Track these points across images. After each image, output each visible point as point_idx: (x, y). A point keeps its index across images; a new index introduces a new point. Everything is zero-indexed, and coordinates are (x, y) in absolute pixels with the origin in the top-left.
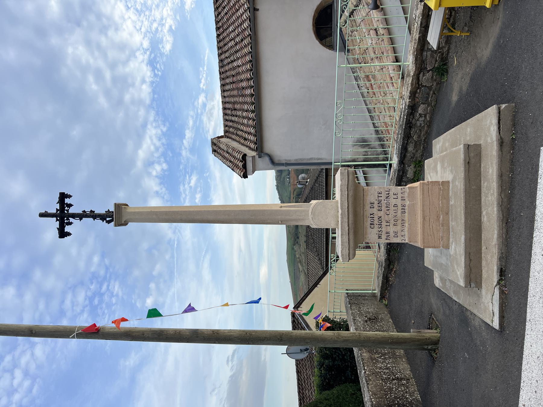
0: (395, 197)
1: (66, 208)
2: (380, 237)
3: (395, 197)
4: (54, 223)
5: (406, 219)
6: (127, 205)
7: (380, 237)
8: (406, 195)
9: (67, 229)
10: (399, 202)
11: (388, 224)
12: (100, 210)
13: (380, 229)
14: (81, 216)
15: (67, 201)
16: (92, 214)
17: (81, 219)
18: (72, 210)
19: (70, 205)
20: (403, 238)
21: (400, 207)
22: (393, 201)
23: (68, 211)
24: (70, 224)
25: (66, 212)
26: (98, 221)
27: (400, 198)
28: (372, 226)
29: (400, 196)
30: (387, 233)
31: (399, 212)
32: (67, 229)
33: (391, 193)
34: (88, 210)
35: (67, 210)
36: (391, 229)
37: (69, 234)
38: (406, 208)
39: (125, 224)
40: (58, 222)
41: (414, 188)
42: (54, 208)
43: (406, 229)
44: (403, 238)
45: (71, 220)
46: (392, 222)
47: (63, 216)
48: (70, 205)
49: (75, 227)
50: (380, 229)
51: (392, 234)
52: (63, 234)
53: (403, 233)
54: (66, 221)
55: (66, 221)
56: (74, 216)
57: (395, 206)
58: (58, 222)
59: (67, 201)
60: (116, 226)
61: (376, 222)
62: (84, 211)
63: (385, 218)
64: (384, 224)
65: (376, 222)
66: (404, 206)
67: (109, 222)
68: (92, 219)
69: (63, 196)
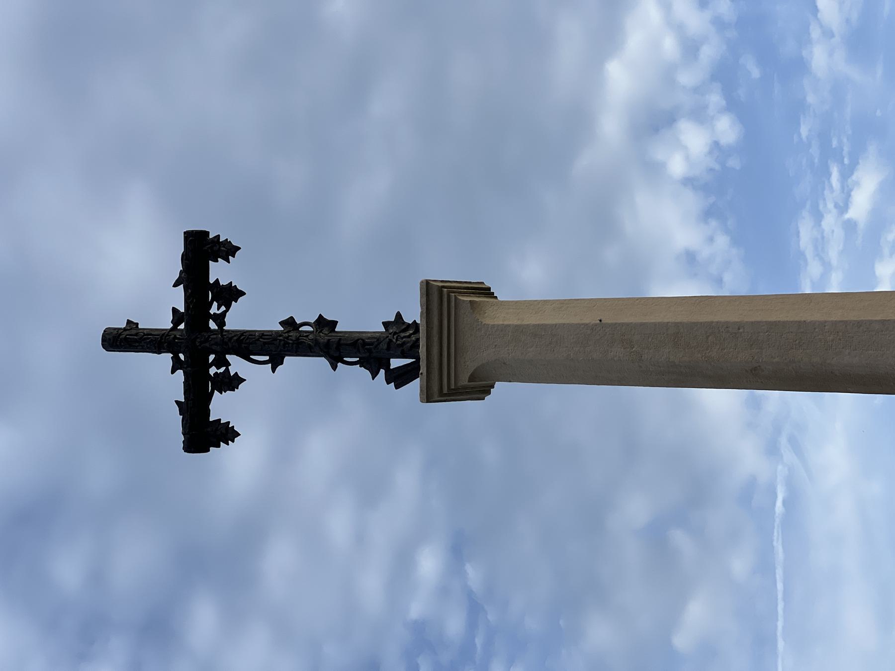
1: (214, 309)
4: (159, 379)
6: (487, 292)
9: (221, 407)
12: (362, 318)
14: (277, 346)
15: (219, 272)
16: (323, 337)
17: (276, 362)
18: (239, 318)
19: (229, 295)
23: (220, 319)
24: (231, 382)
25: (213, 325)
26: (353, 374)
32: (221, 407)
34: (306, 315)
35: (216, 318)
37: (225, 434)
39: (478, 389)
40: (180, 373)
42: (160, 303)
45: (237, 364)
47: (201, 342)
48: (229, 295)
49: (254, 397)
52: (204, 434)
54: (213, 371)
55: (213, 371)
56: (249, 344)
58: (180, 373)
59: (219, 272)
60: (428, 397)
62: (289, 323)
67: (399, 378)
68: (322, 362)
69: (201, 249)
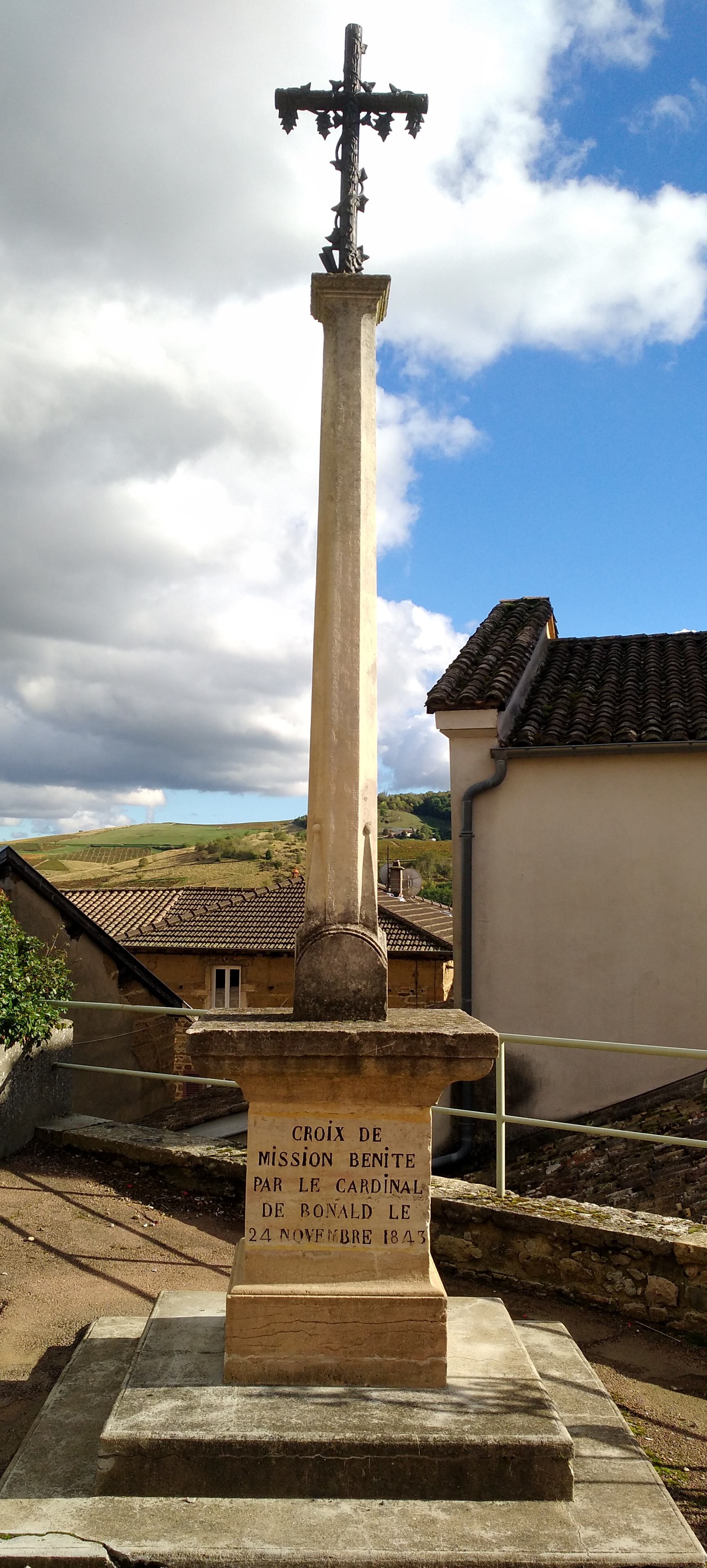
0: (397, 1212)
1: (374, 116)
2: (263, 1157)
3: (397, 1212)
4: (324, 75)
5: (324, 1245)
6: (380, 319)
7: (263, 1157)
8: (402, 1246)
9: (306, 119)
10: (379, 1223)
11: (307, 1185)
12: (365, 231)
13: (290, 1159)
14: (346, 164)
15: (399, 120)
16: (354, 202)
17: (338, 164)
18: (367, 134)
19: (383, 129)
20: (259, 1234)
21: (361, 1225)
22: (381, 1202)
23: (367, 121)
24: (323, 128)
25: (363, 115)
26: (328, 224)
27: (390, 1226)
28: (300, 1134)
29: (400, 1226)
30: (278, 1182)
31: (349, 1224)
32: (306, 119)
33: (408, 1199)
34: (369, 189)
35: (368, 117)
36: (290, 1198)
37: (289, 123)
38: (360, 1246)
39: (319, 309)
40: (329, 88)
41: (425, 1272)
42: (379, 74)
43: (289, 1244)
44: (259, 1234)
45: (336, 133)
46: (312, 1199)
47: (350, 107)
48: (383, 129)
49: (312, 146)
50: (290, 1159)
51: (274, 1197)
52: (290, 103)
53: (275, 1234)
54: (331, 114)
55: (331, 114)
56: (348, 142)
57: (368, 1212)
58: (329, 88)
59: (399, 120)
60: (315, 277)
61: (316, 1147)
62: (363, 177)
63: (327, 1176)
64: (308, 1173)
65: (316, 1147)
66: (366, 1238)
67: (326, 257)
68: (337, 200)
69: (414, 107)
